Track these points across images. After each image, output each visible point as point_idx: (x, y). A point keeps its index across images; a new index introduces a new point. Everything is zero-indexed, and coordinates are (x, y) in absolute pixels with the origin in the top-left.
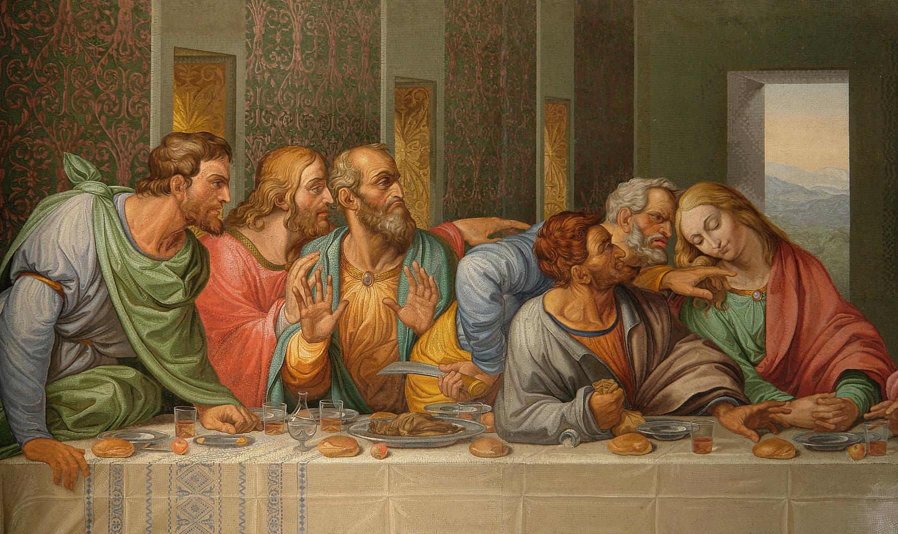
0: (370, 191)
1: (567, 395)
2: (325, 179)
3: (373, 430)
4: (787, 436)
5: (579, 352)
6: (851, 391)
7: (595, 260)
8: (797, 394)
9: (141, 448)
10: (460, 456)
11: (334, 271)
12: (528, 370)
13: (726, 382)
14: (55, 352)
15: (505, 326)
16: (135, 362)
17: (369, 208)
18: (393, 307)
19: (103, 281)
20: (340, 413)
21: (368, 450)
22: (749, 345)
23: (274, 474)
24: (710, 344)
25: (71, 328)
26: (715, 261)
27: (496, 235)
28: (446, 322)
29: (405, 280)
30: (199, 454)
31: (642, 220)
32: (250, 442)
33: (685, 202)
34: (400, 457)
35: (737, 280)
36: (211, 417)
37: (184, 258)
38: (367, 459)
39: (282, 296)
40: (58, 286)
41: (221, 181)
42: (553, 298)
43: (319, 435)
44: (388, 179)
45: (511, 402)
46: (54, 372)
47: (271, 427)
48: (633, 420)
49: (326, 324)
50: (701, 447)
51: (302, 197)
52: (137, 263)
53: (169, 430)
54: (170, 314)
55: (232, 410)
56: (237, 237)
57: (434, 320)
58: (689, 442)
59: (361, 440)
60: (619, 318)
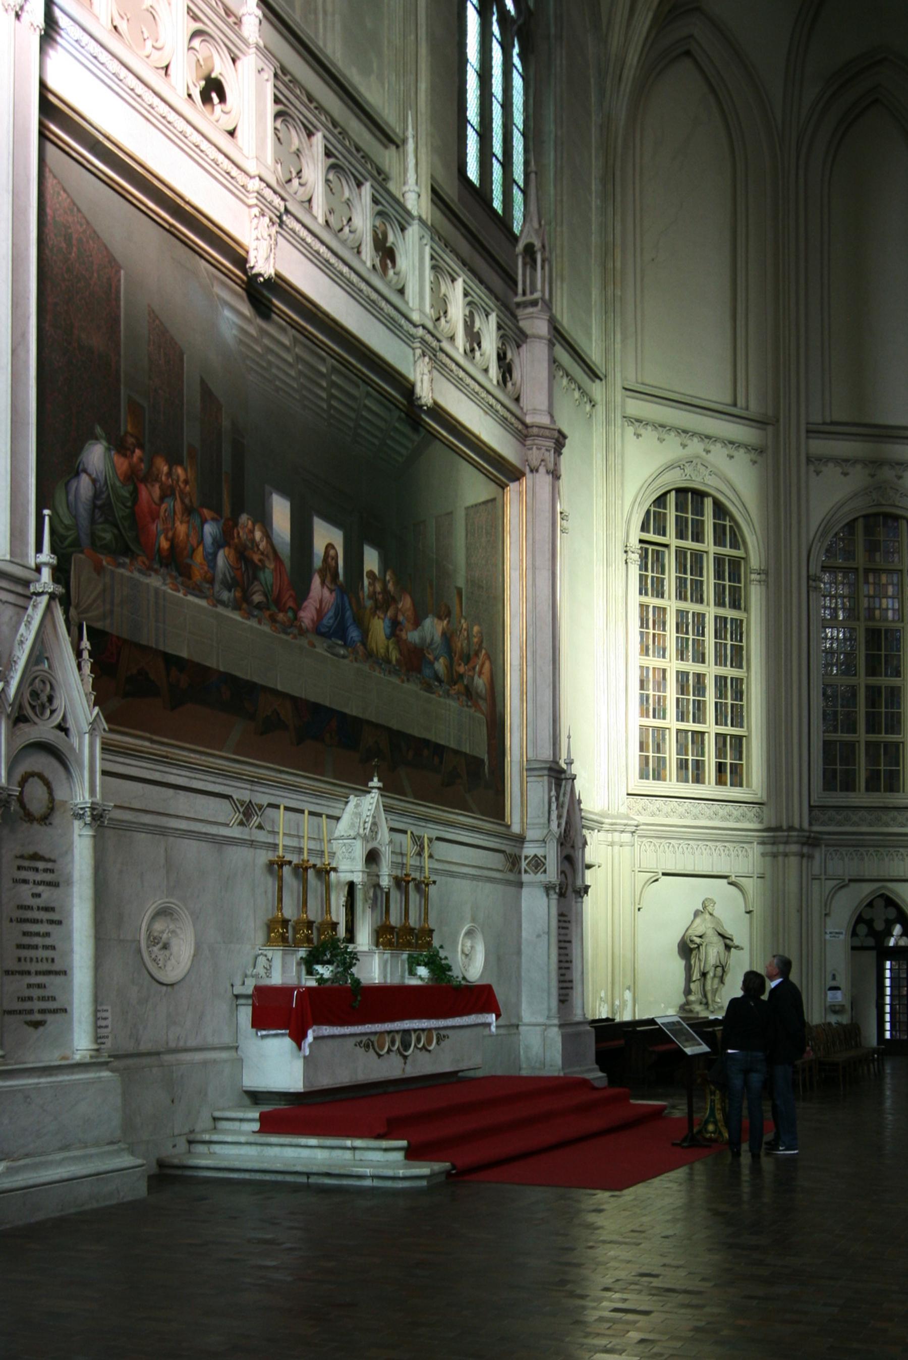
0: (182, 486)
1: (230, 591)
2: (169, 474)
3: (182, 584)
4: (277, 625)
5: (232, 574)
6: (290, 614)
7: (236, 540)
8: (280, 610)
9: (120, 565)
10: (203, 603)
11: (172, 514)
12: (221, 576)
13: (265, 600)
14: (93, 511)
15: (215, 555)
16: (117, 526)
17: (182, 492)
18: (188, 535)
19: (107, 487)
20: (174, 573)
21: (182, 591)
22: (270, 588)
23: (157, 590)
24: (261, 583)
25: (99, 503)
26: (262, 554)
27: (213, 519)
28: (201, 549)
29: (191, 526)
30: (136, 575)
31: (246, 530)
32: (150, 576)
33: (256, 528)
34: (190, 598)
35: (267, 563)
36: (140, 558)
37: (131, 487)
38: (181, 595)
39: (158, 517)
40: (94, 481)
41: (141, 460)
42: (227, 549)
43: (169, 581)
44: (186, 482)
45: (217, 587)
46: (93, 521)
47: (156, 572)
48: (244, 606)
49: (170, 534)
50: (260, 622)
51: (164, 478)
52: (118, 484)
53: (127, 561)
54: (127, 510)
55: (145, 560)
56: (146, 486)
57: (198, 546)
58: (257, 619)
59: (180, 587)
60: (241, 567)
